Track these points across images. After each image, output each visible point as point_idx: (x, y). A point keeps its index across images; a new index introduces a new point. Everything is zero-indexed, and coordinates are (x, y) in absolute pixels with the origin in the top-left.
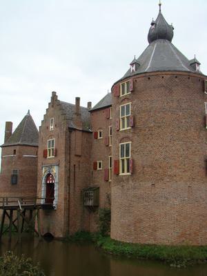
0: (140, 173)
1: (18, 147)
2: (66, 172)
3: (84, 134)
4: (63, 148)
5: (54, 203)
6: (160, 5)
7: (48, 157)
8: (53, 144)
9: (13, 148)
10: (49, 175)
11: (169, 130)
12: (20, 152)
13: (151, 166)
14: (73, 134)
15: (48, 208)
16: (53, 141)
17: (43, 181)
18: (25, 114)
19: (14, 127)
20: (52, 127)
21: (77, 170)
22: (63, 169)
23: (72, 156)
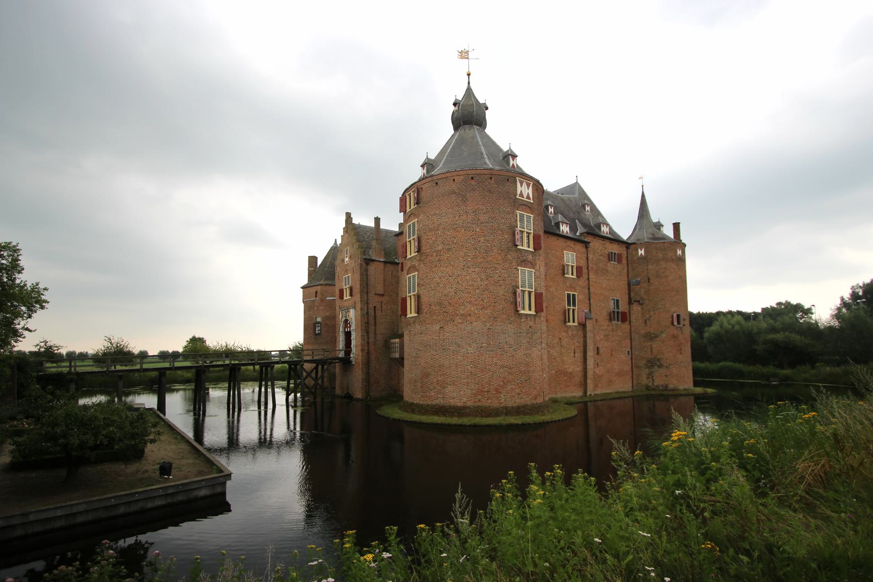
2: (362, 316)
3: (388, 265)
4: (358, 286)
5: (352, 356)
7: (345, 298)
10: (346, 320)
14: (372, 268)
15: (346, 362)
20: (347, 259)
21: (378, 313)
22: (359, 313)
23: (371, 295)
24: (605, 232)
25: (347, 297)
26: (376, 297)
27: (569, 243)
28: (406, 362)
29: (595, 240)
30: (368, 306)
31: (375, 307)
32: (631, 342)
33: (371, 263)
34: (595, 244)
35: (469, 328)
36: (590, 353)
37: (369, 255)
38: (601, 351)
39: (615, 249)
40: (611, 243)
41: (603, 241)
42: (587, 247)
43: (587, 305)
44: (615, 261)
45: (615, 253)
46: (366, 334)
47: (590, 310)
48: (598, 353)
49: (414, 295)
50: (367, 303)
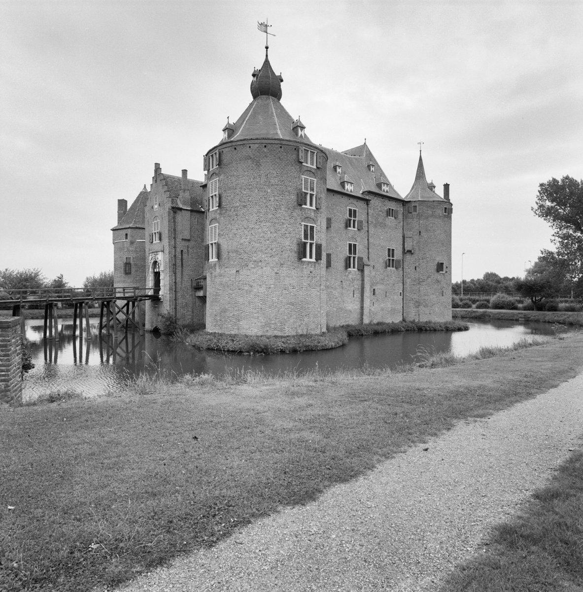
0: (225, 259)
1: (129, 230)
3: (194, 214)
4: (167, 232)
6: (267, 48)
7: (154, 242)
8: (158, 227)
9: (124, 232)
10: (155, 263)
11: (255, 210)
12: (132, 236)
13: (237, 251)
15: (156, 299)
16: (158, 223)
17: (151, 270)
18: (141, 189)
19: (129, 206)
20: (156, 207)
21: (185, 256)
23: (179, 240)
24: (386, 191)
25: (156, 241)
26: (184, 243)
27: (352, 200)
28: (208, 299)
29: (376, 198)
30: (175, 250)
31: (182, 251)
32: (403, 285)
33: (179, 212)
34: (375, 202)
35: (260, 272)
36: (368, 293)
37: (177, 204)
38: (377, 292)
39: (392, 206)
40: (389, 200)
41: (382, 199)
42: (368, 205)
43: (366, 254)
44: (392, 216)
45: (392, 210)
46: (174, 275)
47: (368, 258)
48: (374, 294)
49: (215, 243)
50: (175, 247)
